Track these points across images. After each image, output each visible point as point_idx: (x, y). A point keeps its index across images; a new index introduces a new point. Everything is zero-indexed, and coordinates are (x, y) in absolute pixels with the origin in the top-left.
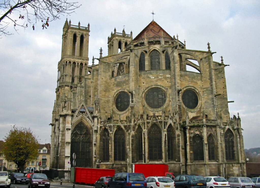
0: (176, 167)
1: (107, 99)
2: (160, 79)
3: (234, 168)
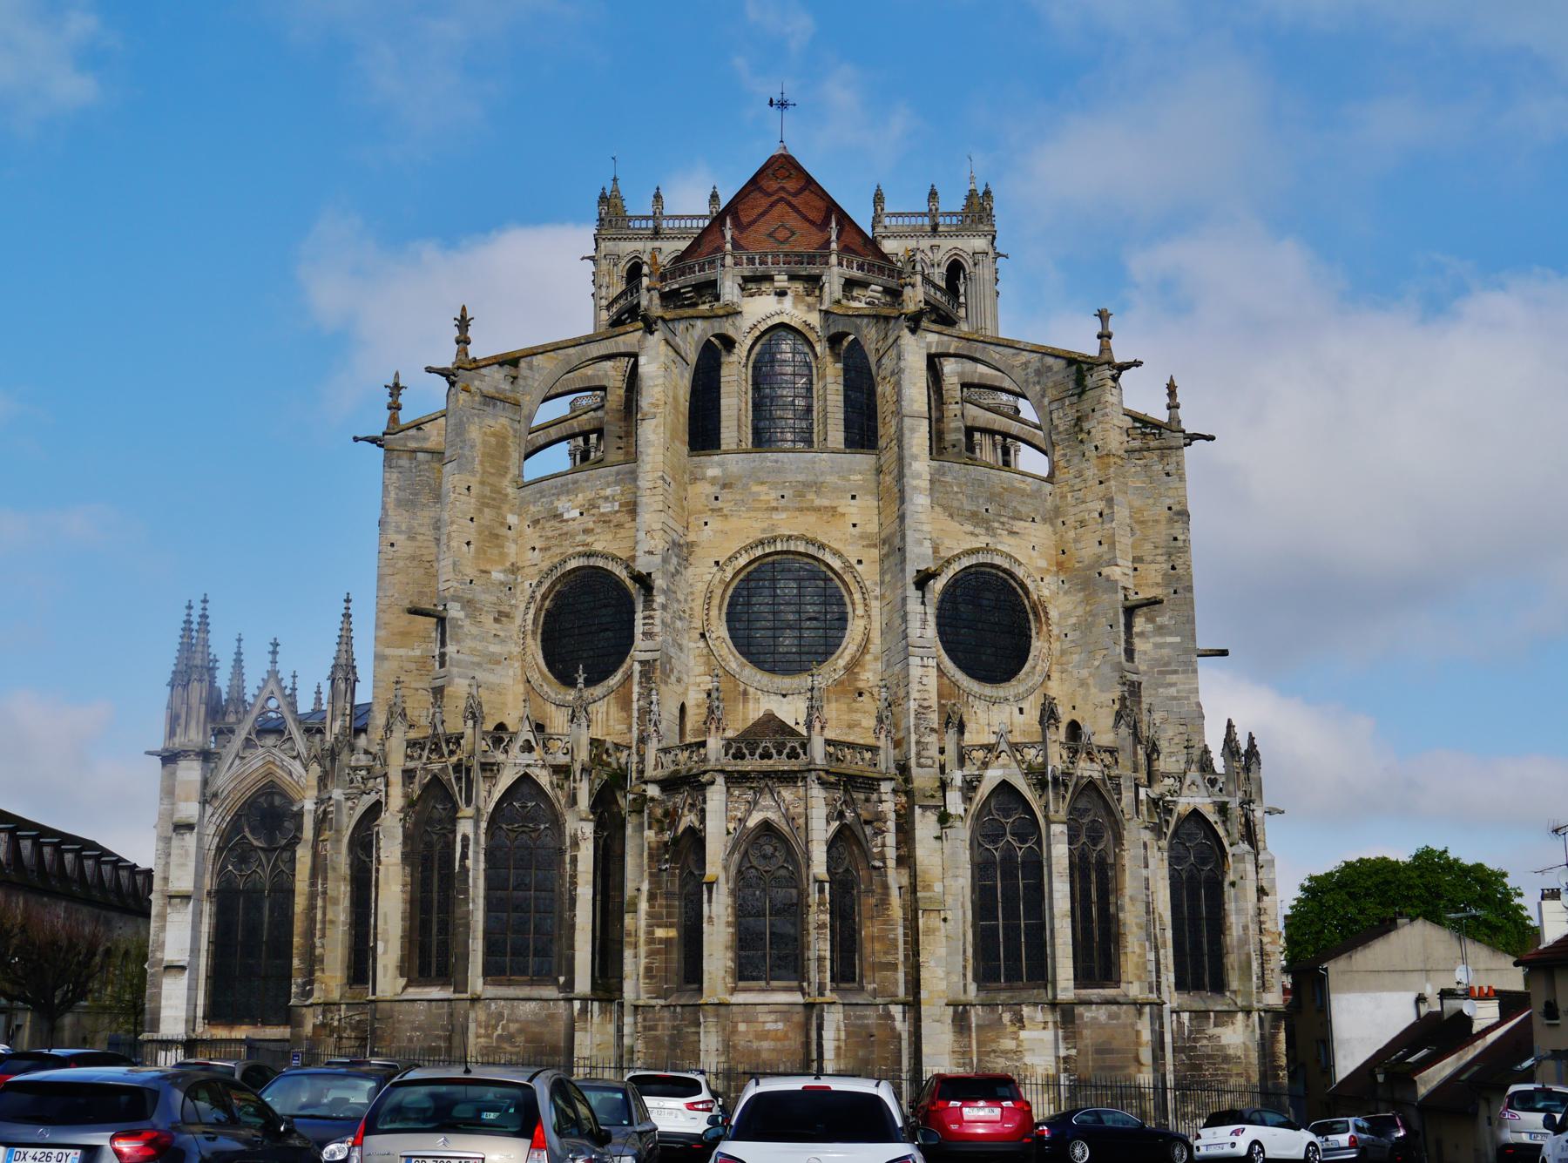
0: (552, 1017)
1: (418, 653)
2: (605, 520)
3: (1023, 1034)
